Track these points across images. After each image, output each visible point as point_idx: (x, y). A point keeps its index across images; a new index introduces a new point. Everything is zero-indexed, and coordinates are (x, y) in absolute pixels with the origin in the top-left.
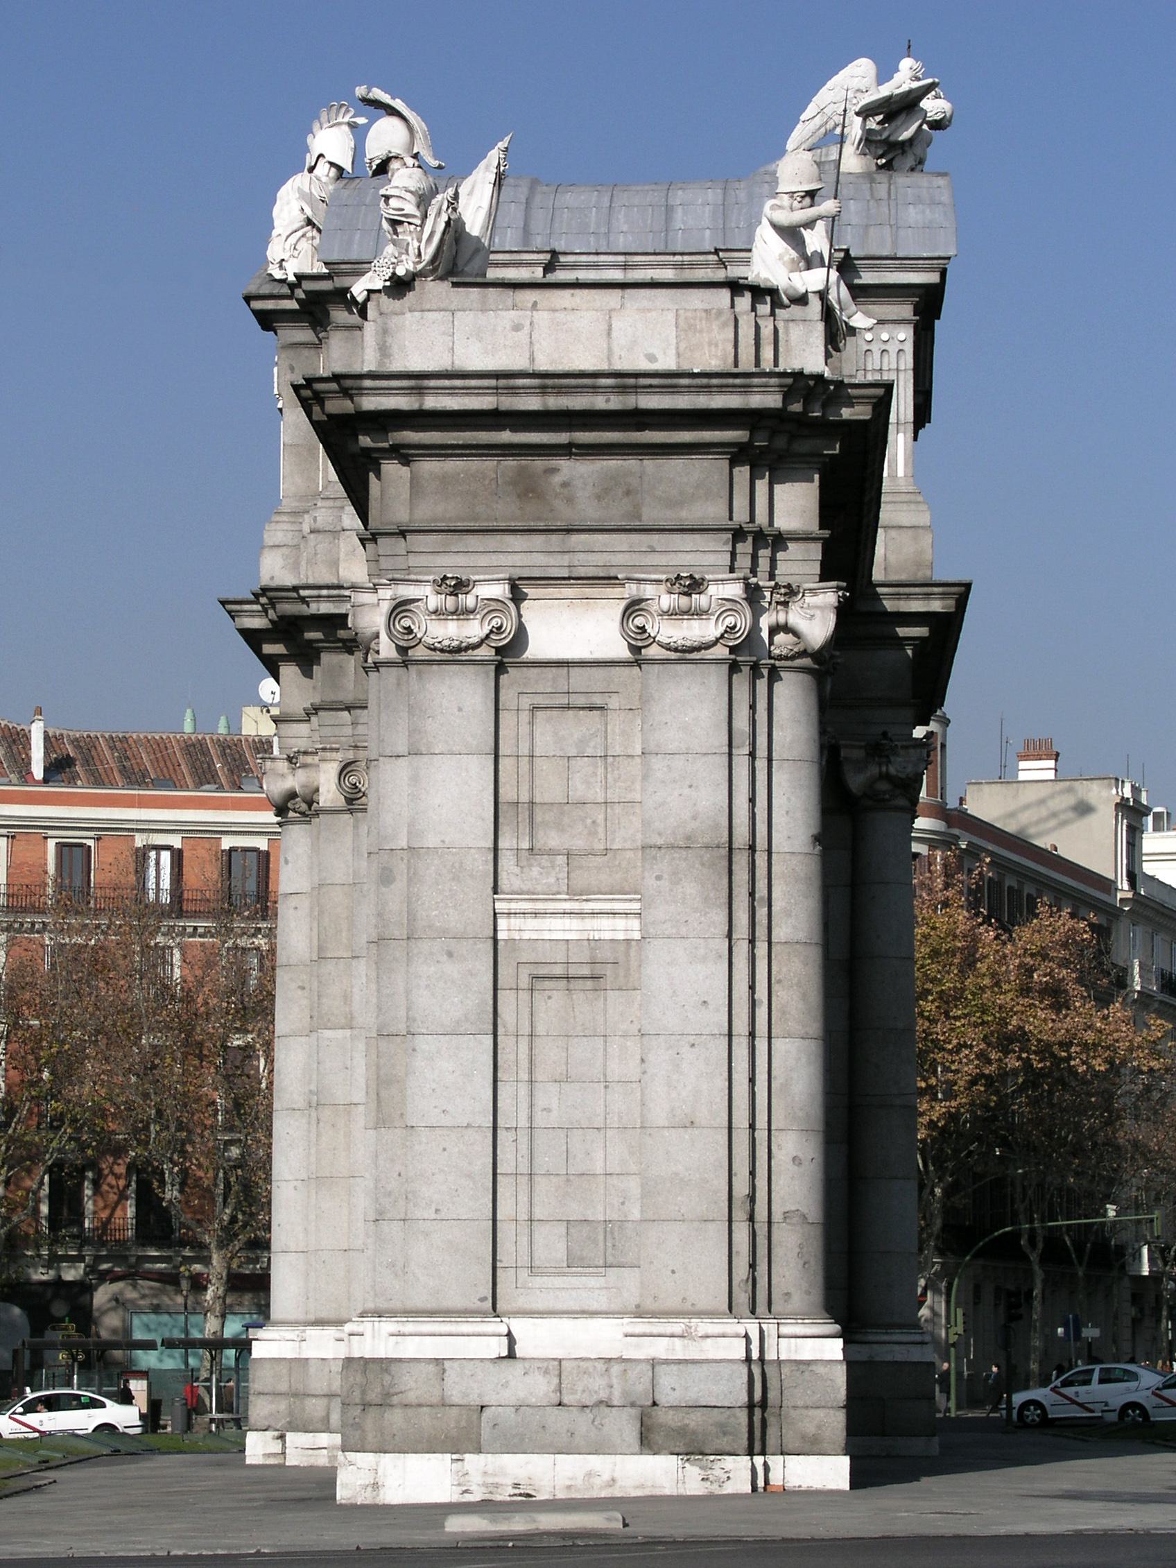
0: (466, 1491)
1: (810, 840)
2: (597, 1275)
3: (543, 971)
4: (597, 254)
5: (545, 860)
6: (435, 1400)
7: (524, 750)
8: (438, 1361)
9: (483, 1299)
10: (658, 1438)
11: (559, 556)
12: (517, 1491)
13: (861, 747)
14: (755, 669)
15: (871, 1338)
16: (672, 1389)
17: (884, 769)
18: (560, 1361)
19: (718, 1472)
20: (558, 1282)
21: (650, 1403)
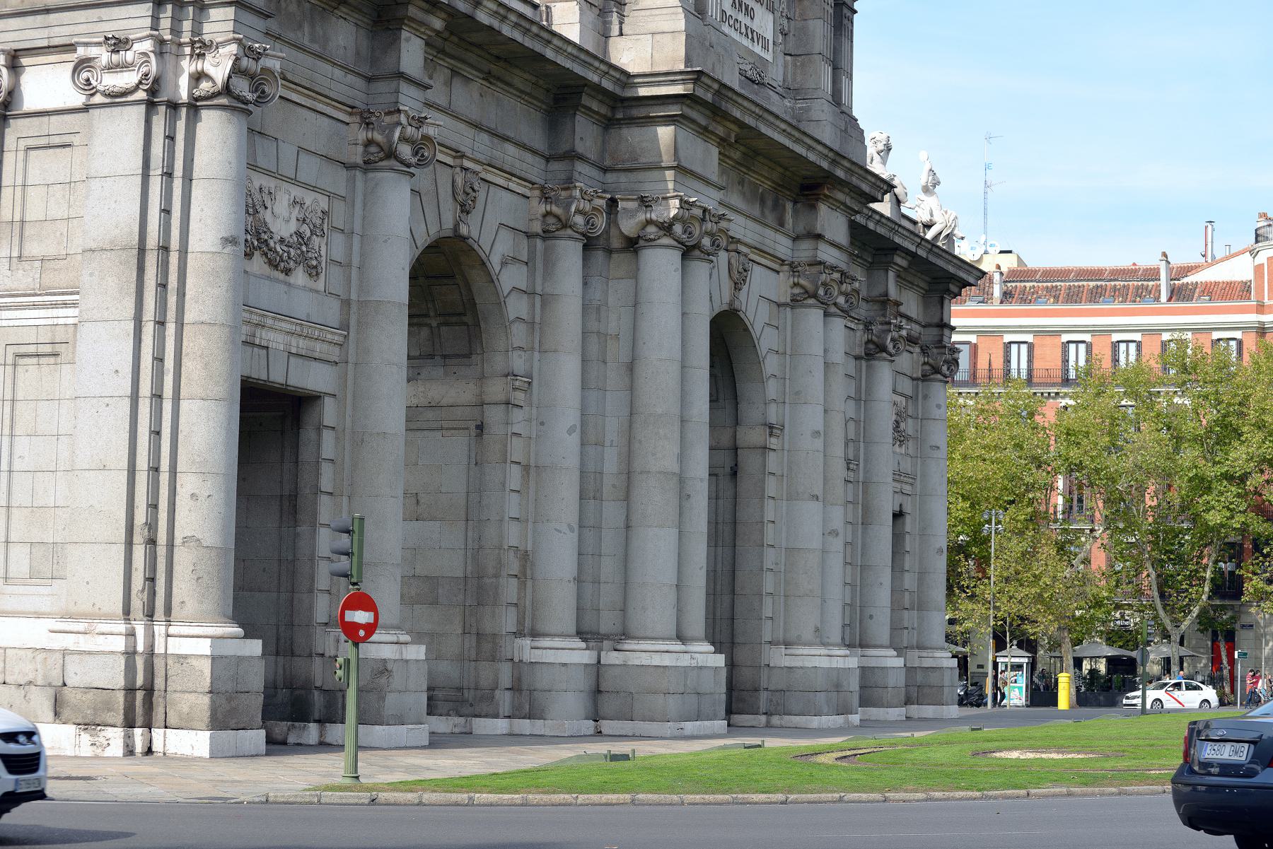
1: (219, 242)
3: (23, 349)
5: (26, 265)
10: (66, 713)
13: (633, 200)
15: (626, 647)
16: (79, 674)
17: (648, 216)
18: (5, 649)
20: (21, 589)
21: (60, 683)
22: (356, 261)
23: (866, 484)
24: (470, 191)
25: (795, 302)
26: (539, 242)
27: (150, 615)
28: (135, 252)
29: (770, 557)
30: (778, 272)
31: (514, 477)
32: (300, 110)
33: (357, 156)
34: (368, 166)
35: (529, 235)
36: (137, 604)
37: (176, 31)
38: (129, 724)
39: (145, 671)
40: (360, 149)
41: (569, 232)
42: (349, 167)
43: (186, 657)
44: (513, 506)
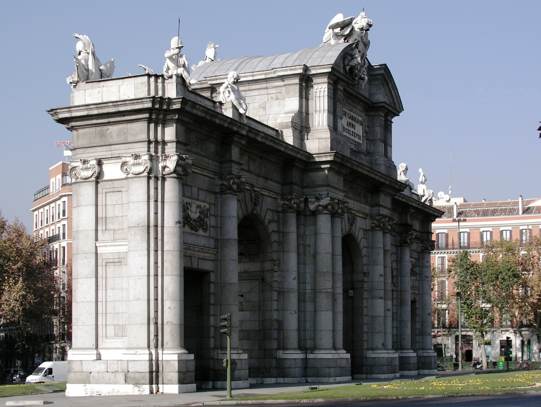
0: (87, 393)
1: (175, 223)
2: (120, 338)
3: (108, 261)
4: (245, 73)
6: (80, 371)
7: (104, 204)
8: (81, 361)
9: (93, 345)
10: (128, 380)
11: (109, 152)
12: (98, 394)
13: (314, 198)
14: (157, 178)
16: (133, 368)
17: (319, 203)
18: (107, 361)
19: (142, 389)
20: (112, 340)
21: (127, 371)
22: (219, 226)
23: (401, 291)
24: (257, 199)
25: (373, 229)
26: (281, 214)
27: (156, 347)
28: (146, 227)
29: (366, 320)
30: (366, 219)
31: (275, 295)
32: (198, 175)
33: (217, 190)
34: (222, 193)
35: (277, 212)
36: (152, 344)
37: (156, 152)
38: (151, 383)
39: (156, 366)
40: (219, 187)
41: (292, 210)
42: (215, 193)
43: (169, 361)
44: (275, 306)
